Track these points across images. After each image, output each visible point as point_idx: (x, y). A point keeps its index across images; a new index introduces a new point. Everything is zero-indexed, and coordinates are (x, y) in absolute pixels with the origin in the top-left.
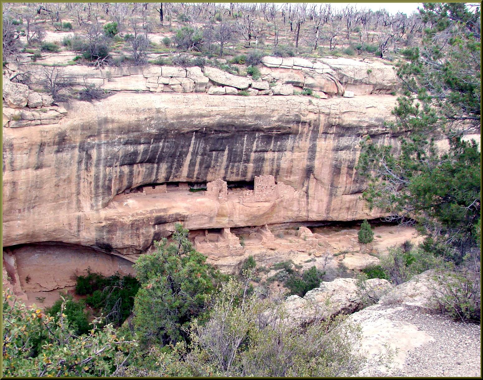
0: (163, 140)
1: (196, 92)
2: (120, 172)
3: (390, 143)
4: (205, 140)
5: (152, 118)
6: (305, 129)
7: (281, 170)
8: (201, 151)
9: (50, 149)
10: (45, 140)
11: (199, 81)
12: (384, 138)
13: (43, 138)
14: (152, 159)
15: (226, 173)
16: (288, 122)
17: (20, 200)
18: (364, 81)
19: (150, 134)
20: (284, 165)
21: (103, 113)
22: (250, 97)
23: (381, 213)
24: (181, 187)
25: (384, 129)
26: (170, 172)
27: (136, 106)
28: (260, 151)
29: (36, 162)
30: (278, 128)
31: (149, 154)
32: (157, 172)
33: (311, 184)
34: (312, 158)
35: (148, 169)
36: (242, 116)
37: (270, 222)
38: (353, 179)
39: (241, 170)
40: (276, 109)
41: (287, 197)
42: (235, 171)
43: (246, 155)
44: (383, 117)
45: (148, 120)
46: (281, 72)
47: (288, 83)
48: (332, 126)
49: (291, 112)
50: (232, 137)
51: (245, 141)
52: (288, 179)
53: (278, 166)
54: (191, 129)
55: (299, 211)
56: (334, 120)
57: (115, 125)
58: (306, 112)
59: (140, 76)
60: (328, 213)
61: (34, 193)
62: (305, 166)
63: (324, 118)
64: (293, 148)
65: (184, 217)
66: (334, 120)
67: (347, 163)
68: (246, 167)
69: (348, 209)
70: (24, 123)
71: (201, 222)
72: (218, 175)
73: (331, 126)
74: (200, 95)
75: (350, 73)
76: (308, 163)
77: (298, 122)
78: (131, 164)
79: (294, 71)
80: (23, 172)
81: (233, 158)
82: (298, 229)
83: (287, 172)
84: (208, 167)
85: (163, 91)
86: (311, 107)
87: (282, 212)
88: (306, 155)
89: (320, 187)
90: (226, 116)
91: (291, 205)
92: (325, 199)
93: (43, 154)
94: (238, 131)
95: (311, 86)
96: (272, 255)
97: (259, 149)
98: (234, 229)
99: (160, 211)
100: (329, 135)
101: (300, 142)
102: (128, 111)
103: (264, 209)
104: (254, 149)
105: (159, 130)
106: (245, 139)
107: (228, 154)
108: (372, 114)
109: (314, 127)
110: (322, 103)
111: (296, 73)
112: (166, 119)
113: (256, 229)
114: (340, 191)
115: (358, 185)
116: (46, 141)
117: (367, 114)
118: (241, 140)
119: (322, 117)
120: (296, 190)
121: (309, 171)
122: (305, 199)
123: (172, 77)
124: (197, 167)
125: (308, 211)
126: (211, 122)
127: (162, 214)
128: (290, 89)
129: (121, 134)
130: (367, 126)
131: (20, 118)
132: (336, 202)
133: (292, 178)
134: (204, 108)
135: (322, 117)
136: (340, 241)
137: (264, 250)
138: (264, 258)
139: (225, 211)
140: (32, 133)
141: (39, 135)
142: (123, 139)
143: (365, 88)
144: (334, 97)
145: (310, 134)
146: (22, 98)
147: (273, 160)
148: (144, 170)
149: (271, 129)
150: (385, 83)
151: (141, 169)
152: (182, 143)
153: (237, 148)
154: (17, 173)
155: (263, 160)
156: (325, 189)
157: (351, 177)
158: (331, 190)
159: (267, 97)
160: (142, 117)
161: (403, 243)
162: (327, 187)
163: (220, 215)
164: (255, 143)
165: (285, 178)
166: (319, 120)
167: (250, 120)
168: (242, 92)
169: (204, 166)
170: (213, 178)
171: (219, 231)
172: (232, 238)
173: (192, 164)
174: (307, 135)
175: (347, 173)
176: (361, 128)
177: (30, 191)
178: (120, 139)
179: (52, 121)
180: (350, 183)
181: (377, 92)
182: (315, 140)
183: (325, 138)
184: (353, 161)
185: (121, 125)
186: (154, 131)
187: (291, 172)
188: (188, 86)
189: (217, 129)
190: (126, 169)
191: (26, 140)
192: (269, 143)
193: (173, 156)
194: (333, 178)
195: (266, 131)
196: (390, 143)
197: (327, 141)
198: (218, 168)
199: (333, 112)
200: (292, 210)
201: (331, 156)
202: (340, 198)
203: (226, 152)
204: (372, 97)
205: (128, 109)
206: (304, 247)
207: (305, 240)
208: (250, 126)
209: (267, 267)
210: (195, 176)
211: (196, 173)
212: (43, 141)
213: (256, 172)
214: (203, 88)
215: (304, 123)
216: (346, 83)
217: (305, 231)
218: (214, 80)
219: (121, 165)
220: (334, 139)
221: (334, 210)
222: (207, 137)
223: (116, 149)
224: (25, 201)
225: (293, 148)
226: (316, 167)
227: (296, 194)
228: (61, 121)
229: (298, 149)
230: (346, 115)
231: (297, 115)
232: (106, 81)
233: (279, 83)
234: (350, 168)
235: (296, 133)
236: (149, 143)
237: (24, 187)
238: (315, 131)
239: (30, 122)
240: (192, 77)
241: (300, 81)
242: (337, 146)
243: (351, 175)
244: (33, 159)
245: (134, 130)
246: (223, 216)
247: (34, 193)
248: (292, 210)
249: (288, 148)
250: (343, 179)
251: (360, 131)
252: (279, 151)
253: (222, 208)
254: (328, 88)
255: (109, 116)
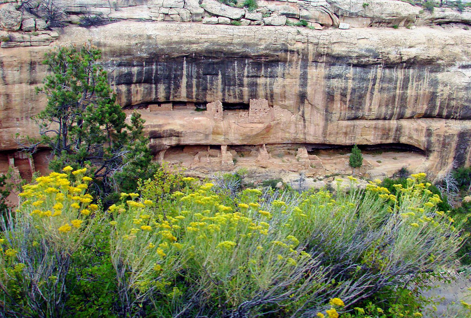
0: (155, 64)
1: (193, 21)
2: (117, 90)
3: (384, 73)
4: (196, 64)
5: (143, 44)
6: (294, 58)
7: (274, 95)
8: (194, 74)
9: (41, 67)
10: (34, 59)
11: (195, 11)
12: (377, 68)
13: (32, 58)
14: (147, 80)
15: (224, 95)
16: (276, 50)
17: (16, 110)
18: (359, 14)
19: (141, 58)
20: (277, 90)
21: (97, 38)
22: (241, 27)
23: (381, 139)
24: (188, 107)
25: (376, 60)
26: (170, 93)
27: (128, 32)
28: (252, 77)
29: (29, 78)
30: (266, 56)
31: (144, 75)
32: (156, 92)
33: (306, 109)
34: (304, 85)
35: (147, 88)
36: (231, 44)
37: (267, 142)
38: (347, 106)
39: (237, 93)
40: (263, 38)
41: (284, 120)
42: (232, 94)
43: (239, 79)
44: (374, 48)
45: (139, 45)
46: (276, 5)
47: (283, 14)
48: (322, 55)
49: (278, 42)
50: (222, 62)
51: (236, 67)
52: (283, 103)
53: (272, 91)
54: (181, 55)
55: (296, 133)
56: (323, 50)
57: (108, 49)
58: (293, 42)
59: (145, 6)
60: (325, 137)
61: (30, 105)
62: (297, 92)
63: (312, 48)
64: (284, 74)
65: (178, 133)
66: (323, 50)
67: (339, 90)
68: (241, 91)
69: (346, 133)
70: (13, 44)
71: (197, 138)
72: (217, 97)
73: (321, 55)
74: (194, 24)
75: (346, 6)
76: (301, 89)
77: (286, 51)
78: (129, 83)
79: (289, 4)
80: (17, 86)
81: (228, 82)
82: (297, 150)
83: (281, 97)
84: (205, 89)
85: (164, 20)
86: (298, 37)
87: (280, 134)
88: (298, 81)
89: (315, 112)
90: (213, 43)
91: (289, 128)
92: (322, 123)
93: (36, 72)
94: (228, 58)
95: (307, 18)
96: (262, 173)
97: (250, 75)
98: (231, 147)
99: (155, 126)
100: (319, 64)
101: (290, 69)
102: (120, 36)
103: (257, 130)
104: (246, 74)
105: (150, 54)
106: (236, 64)
107: (222, 78)
108: (363, 45)
109: (303, 56)
110: (316, 33)
111: (291, 6)
112: (156, 45)
113: (256, 147)
114: (335, 116)
115: (353, 112)
116: (36, 60)
117: (357, 45)
118: (232, 66)
119: (311, 47)
120: (293, 113)
121: (302, 97)
122: (302, 122)
123: (171, 8)
124: (194, 89)
125: (305, 134)
126: (200, 48)
127: (156, 129)
128: (283, 19)
129: (113, 57)
130: (357, 57)
131: (10, 40)
132: (331, 127)
133: (287, 103)
134: (194, 35)
135: (311, 47)
136: (335, 164)
137: (255, 168)
138: (253, 175)
139: (220, 130)
140: (23, 53)
141: (29, 55)
142: (116, 61)
143: (362, 21)
144: (331, 28)
145: (300, 63)
146: (13, 22)
147: (266, 85)
148: (143, 89)
149: (260, 56)
150: (384, 16)
151: (139, 89)
152: (175, 67)
153: (229, 73)
154: (10, 86)
155: (256, 84)
156: (321, 114)
157: (346, 104)
158: (326, 115)
159: (257, 27)
160: (133, 42)
161: (400, 169)
162: (322, 113)
163: (215, 133)
164: (246, 69)
165: (280, 103)
166: (308, 49)
167: (238, 47)
168: (235, 22)
169: (201, 88)
170: (212, 99)
171: (218, 147)
172: (226, 156)
173: (189, 86)
174: (297, 63)
175: (341, 100)
176: (351, 58)
177: (25, 103)
178: (113, 61)
179: (42, 43)
180: (345, 109)
181: (377, 24)
182: (306, 68)
183: (316, 66)
184: (346, 89)
185: (112, 49)
186: (145, 55)
187: (285, 97)
188: (185, 16)
189: (206, 55)
190: (123, 88)
191: (16, 59)
192: (259, 69)
193: (168, 78)
194: (327, 104)
195: (254, 58)
196: (384, 73)
197: (318, 69)
198: (215, 91)
199: (321, 42)
200: (289, 133)
201: (323, 83)
202: (336, 124)
203: (220, 76)
204: (370, 30)
205: (120, 35)
206: (297, 167)
207: (298, 160)
208: (239, 53)
209: (256, 183)
210: (194, 97)
211: (194, 94)
212: (33, 60)
213: (251, 95)
214: (199, 18)
215: (292, 52)
216: (342, 16)
217: (303, 153)
218: (209, 11)
219: (118, 84)
220: (325, 68)
221: (330, 134)
222: (198, 62)
223: (110, 70)
224: (22, 112)
225: (284, 74)
226: (309, 93)
227: (293, 118)
228: (52, 44)
229: (289, 76)
230: (335, 45)
231: (283, 44)
232: (113, 10)
233: (274, 15)
234: (344, 95)
235: (285, 61)
236: (142, 65)
237: (18, 99)
238: (305, 59)
239: (19, 43)
240: (188, 8)
241: (295, 13)
242: (328, 74)
243: (345, 102)
244: (25, 75)
245: (126, 53)
246: (218, 134)
247: (30, 105)
248: (289, 133)
249: (278, 74)
250: (337, 105)
251: (350, 61)
252: (270, 77)
253: (217, 127)
254: (322, 19)
255: (102, 41)
